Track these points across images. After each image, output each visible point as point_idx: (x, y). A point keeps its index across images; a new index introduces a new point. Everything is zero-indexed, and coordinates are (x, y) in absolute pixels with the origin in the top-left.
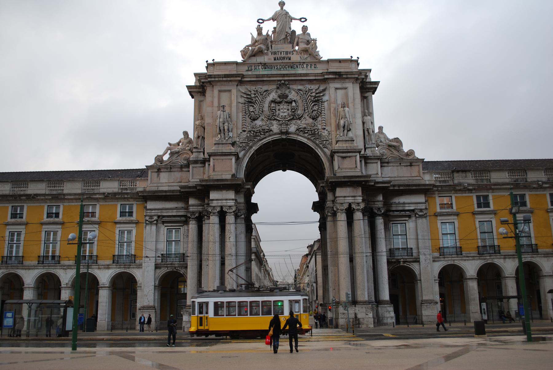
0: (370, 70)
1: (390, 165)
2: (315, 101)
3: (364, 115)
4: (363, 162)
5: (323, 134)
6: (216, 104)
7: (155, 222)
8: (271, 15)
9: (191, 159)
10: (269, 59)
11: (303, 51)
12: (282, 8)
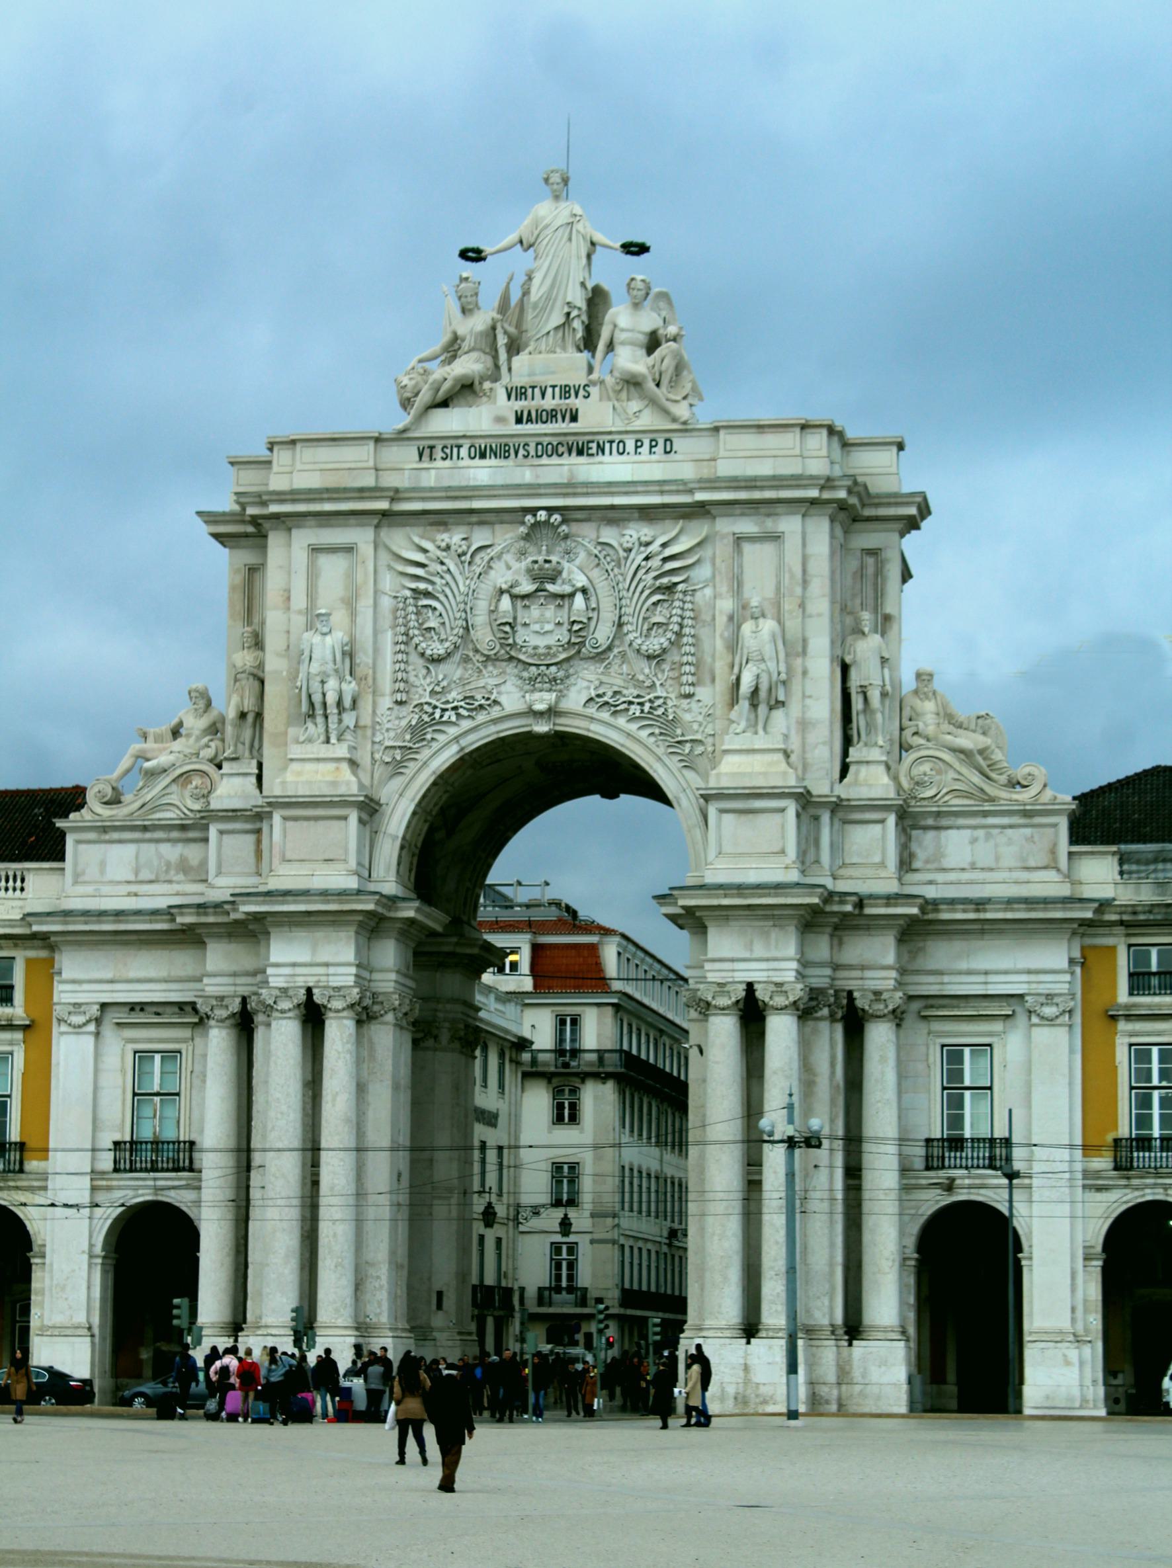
1: (944, 822)
5: (687, 717)
6: (299, 600)
7: (92, 1027)
9: (215, 804)
10: (500, 420)
11: (628, 382)
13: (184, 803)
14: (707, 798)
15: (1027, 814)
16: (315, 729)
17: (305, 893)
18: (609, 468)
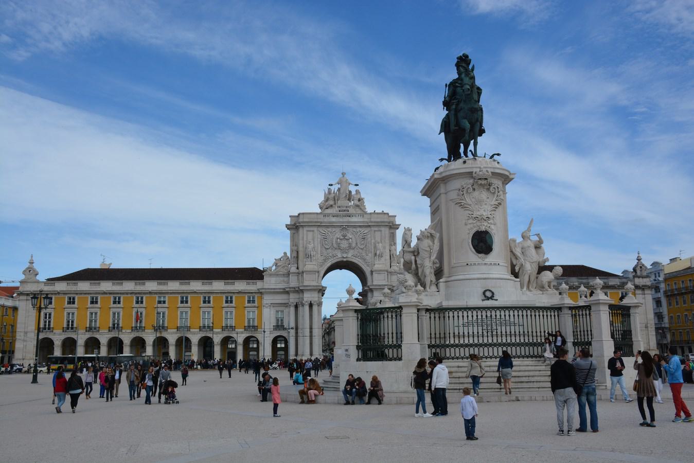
0: (395, 216)
2: (363, 238)
3: (391, 245)
4: (389, 274)
5: (367, 258)
8: (337, 181)
10: (337, 211)
12: (343, 176)
16: (309, 260)
17: (309, 286)
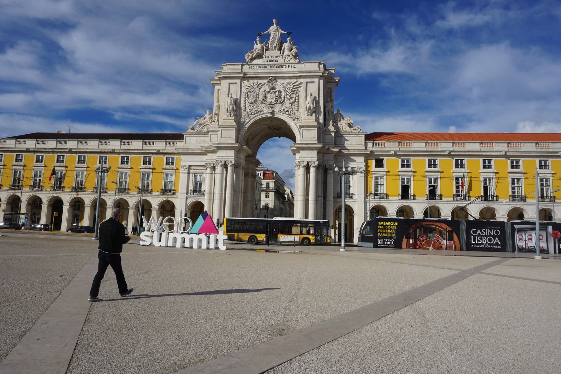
6: (227, 93)
10: (264, 61)
13: (205, 130)
14: (300, 127)
15: (357, 134)
18: (284, 70)
